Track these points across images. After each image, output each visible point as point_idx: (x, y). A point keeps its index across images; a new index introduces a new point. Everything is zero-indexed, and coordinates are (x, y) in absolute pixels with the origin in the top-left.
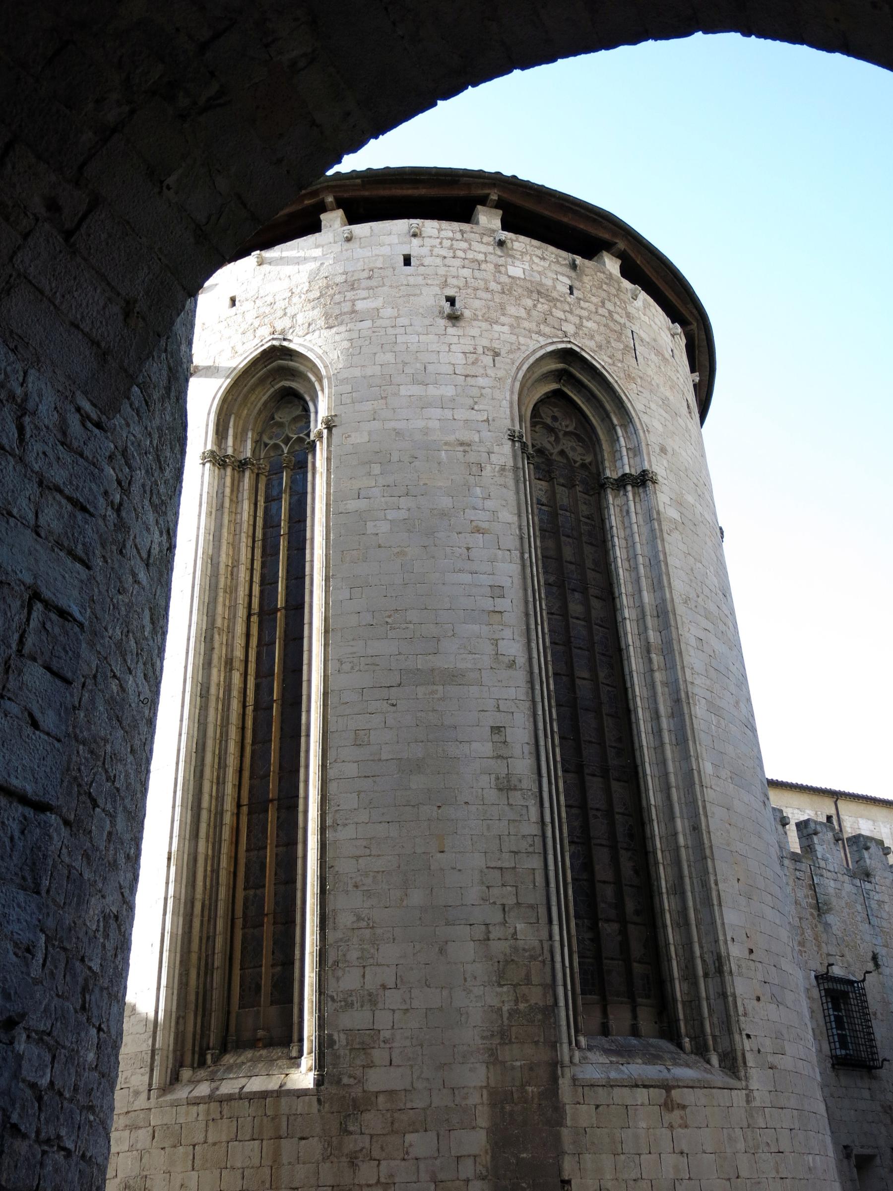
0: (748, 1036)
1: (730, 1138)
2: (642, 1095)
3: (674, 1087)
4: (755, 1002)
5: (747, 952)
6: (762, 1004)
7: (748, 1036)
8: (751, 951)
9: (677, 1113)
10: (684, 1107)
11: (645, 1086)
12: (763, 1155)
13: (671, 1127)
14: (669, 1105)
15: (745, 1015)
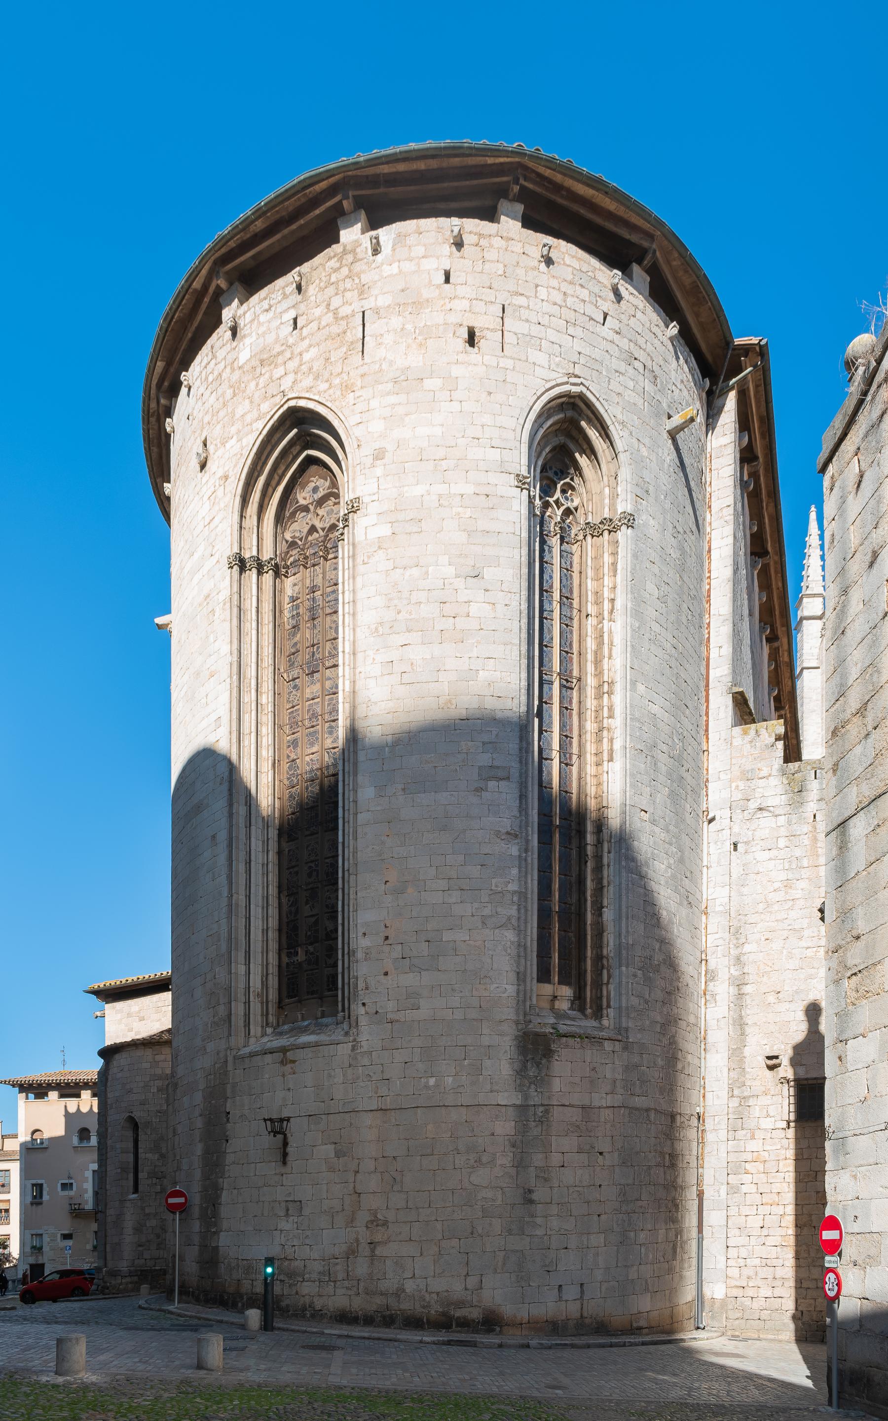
0: (364, 1004)
1: (330, 1076)
2: (268, 1058)
3: (289, 1050)
4: (382, 976)
5: (383, 939)
6: (389, 977)
7: (364, 1004)
8: (387, 938)
9: (289, 1066)
10: (294, 1062)
11: (271, 1053)
12: (362, 1084)
13: (283, 1076)
14: (283, 1063)
15: (367, 988)
